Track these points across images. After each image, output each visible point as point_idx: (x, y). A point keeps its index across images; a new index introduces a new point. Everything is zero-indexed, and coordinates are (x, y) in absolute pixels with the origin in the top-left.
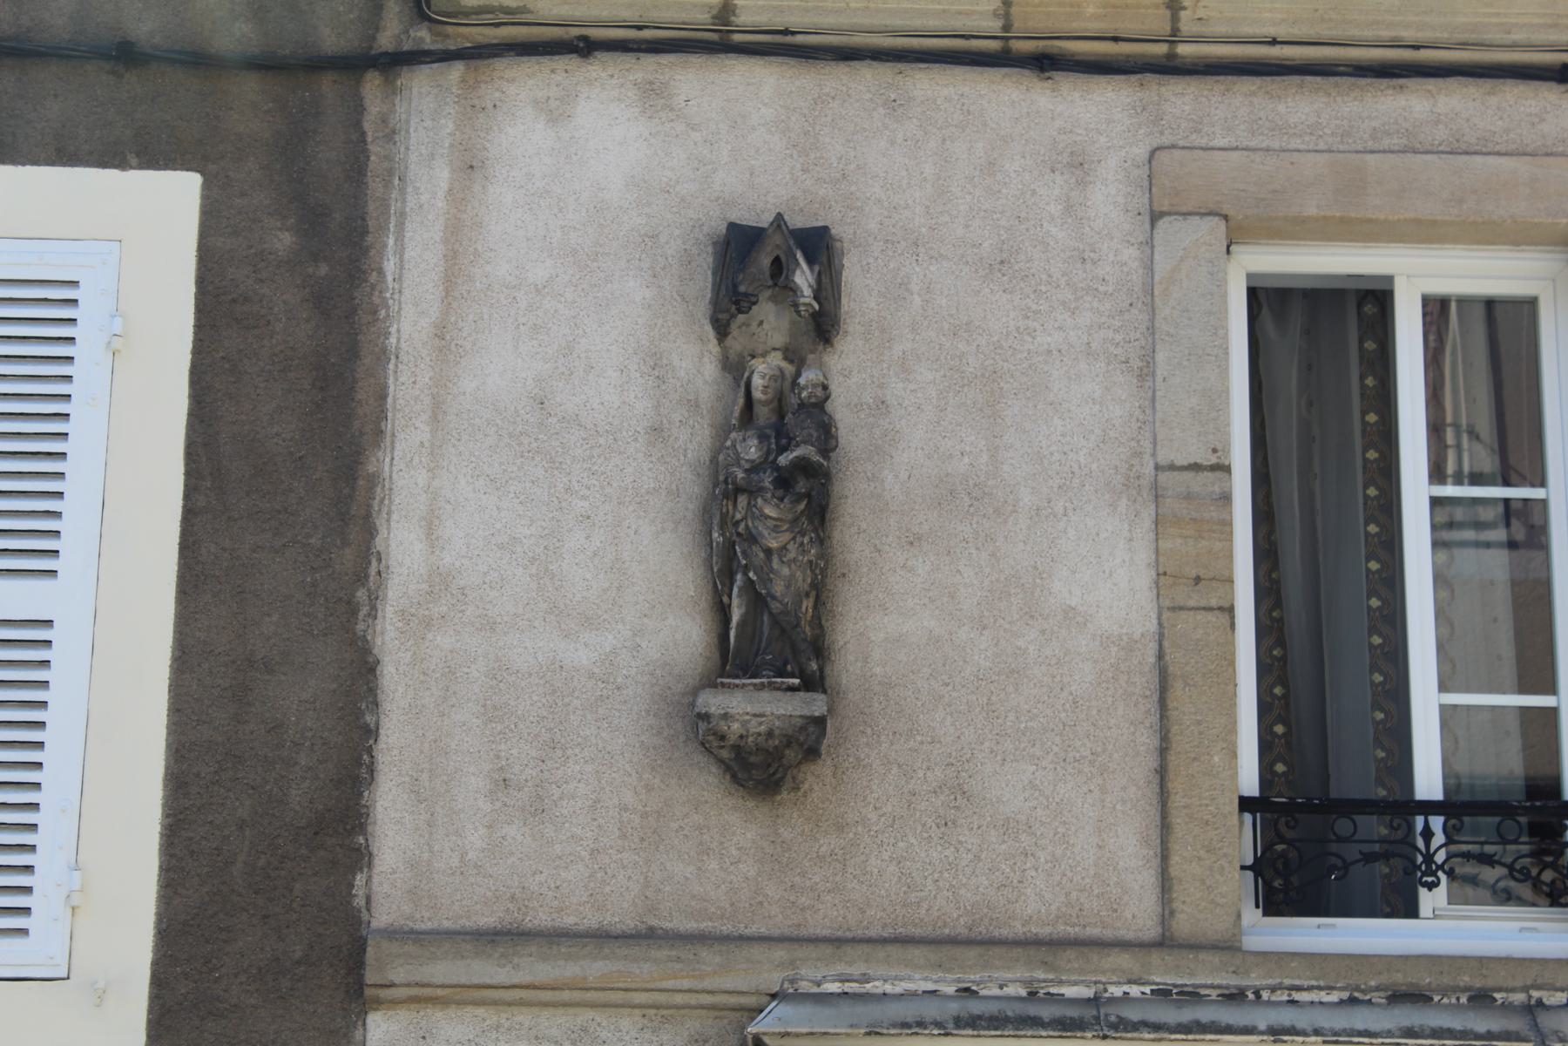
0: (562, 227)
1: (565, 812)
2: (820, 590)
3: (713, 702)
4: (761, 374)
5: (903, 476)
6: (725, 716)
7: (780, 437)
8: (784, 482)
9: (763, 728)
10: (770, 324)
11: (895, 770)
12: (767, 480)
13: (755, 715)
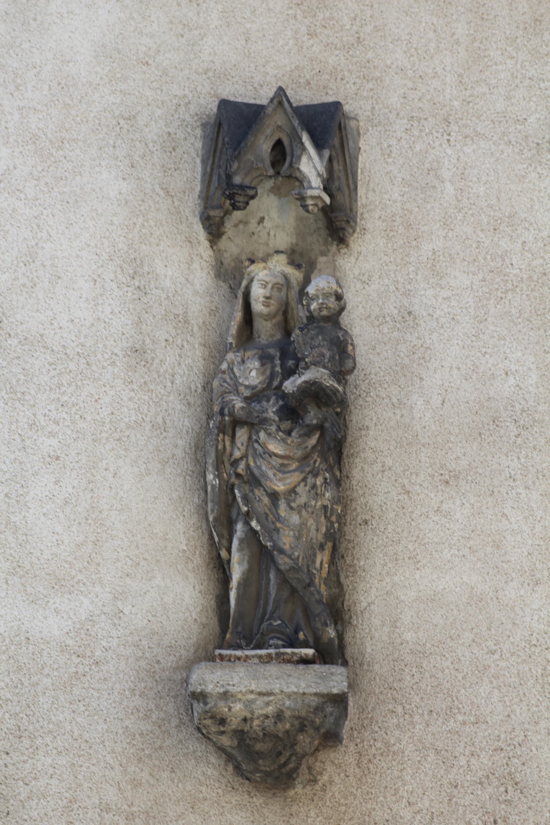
0: (20, 109)
1: (34, 814)
2: (336, 541)
3: (211, 679)
4: (264, 281)
5: (436, 401)
6: (225, 695)
7: (287, 358)
8: (291, 412)
9: (270, 710)
10: (273, 220)
11: (432, 757)
12: (271, 409)
13: (261, 694)
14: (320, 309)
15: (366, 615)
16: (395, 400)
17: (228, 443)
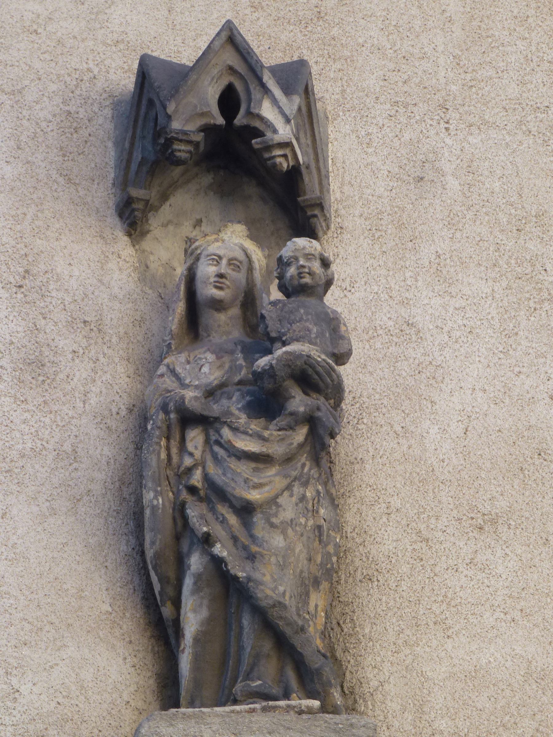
5: (456, 429)
14: (300, 275)
15: (379, 697)
16: (398, 428)
17: (174, 451)
